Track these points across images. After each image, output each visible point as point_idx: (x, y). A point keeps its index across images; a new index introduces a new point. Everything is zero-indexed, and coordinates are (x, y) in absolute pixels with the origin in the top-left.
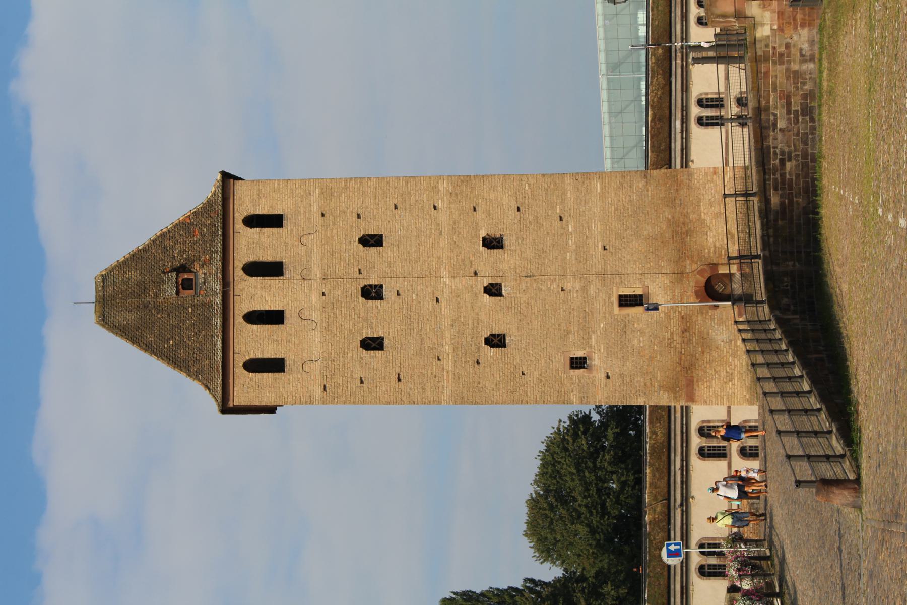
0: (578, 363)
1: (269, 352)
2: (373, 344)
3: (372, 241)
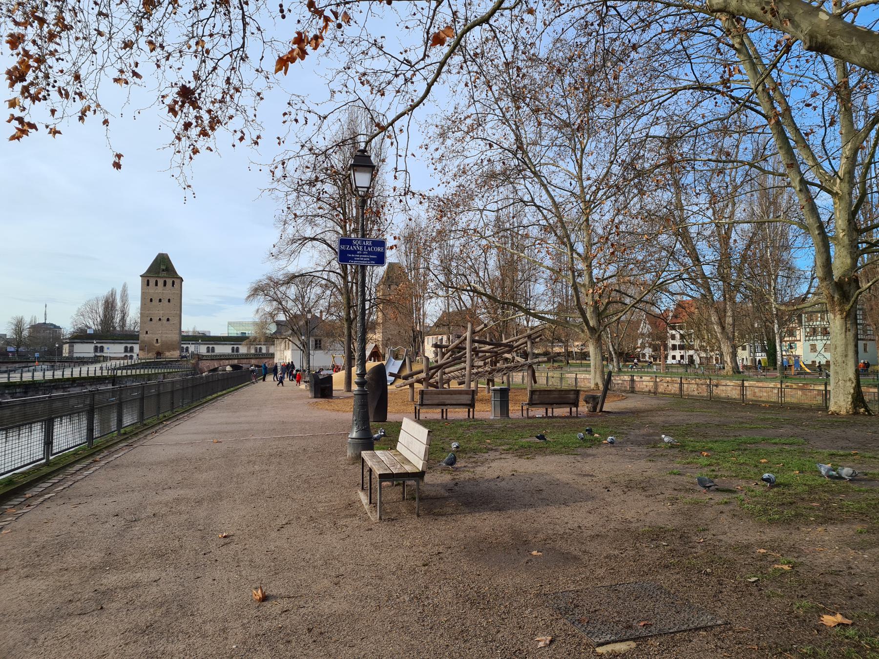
0: (147, 333)
1: (150, 284)
2: (151, 300)
3: (169, 301)
